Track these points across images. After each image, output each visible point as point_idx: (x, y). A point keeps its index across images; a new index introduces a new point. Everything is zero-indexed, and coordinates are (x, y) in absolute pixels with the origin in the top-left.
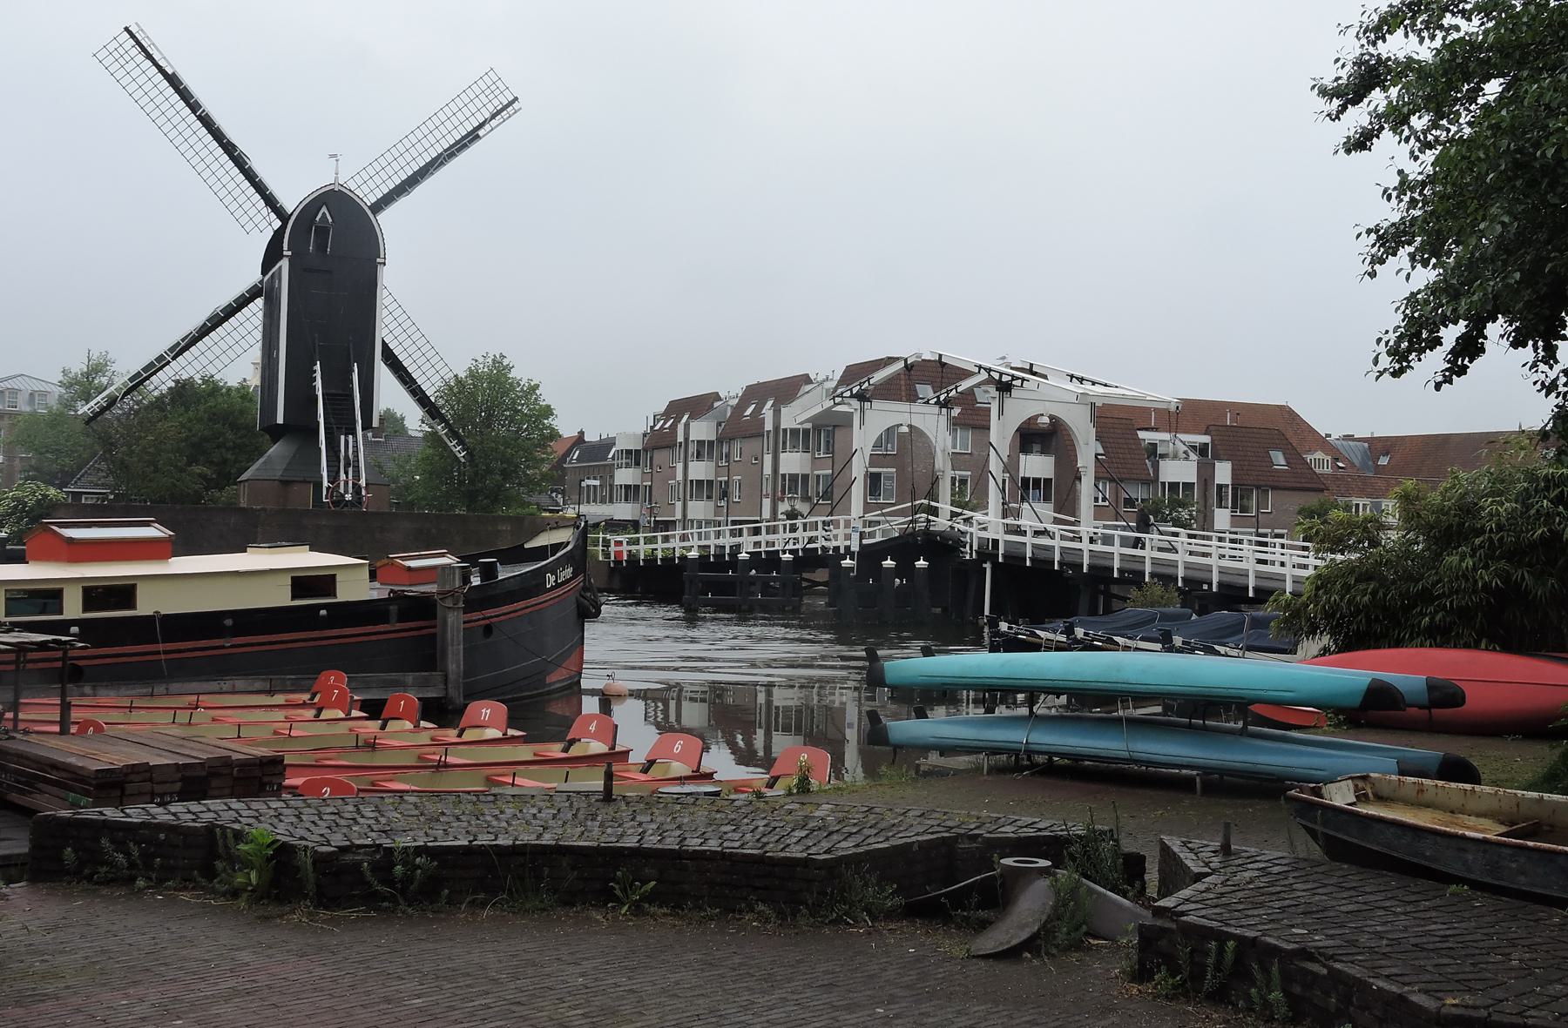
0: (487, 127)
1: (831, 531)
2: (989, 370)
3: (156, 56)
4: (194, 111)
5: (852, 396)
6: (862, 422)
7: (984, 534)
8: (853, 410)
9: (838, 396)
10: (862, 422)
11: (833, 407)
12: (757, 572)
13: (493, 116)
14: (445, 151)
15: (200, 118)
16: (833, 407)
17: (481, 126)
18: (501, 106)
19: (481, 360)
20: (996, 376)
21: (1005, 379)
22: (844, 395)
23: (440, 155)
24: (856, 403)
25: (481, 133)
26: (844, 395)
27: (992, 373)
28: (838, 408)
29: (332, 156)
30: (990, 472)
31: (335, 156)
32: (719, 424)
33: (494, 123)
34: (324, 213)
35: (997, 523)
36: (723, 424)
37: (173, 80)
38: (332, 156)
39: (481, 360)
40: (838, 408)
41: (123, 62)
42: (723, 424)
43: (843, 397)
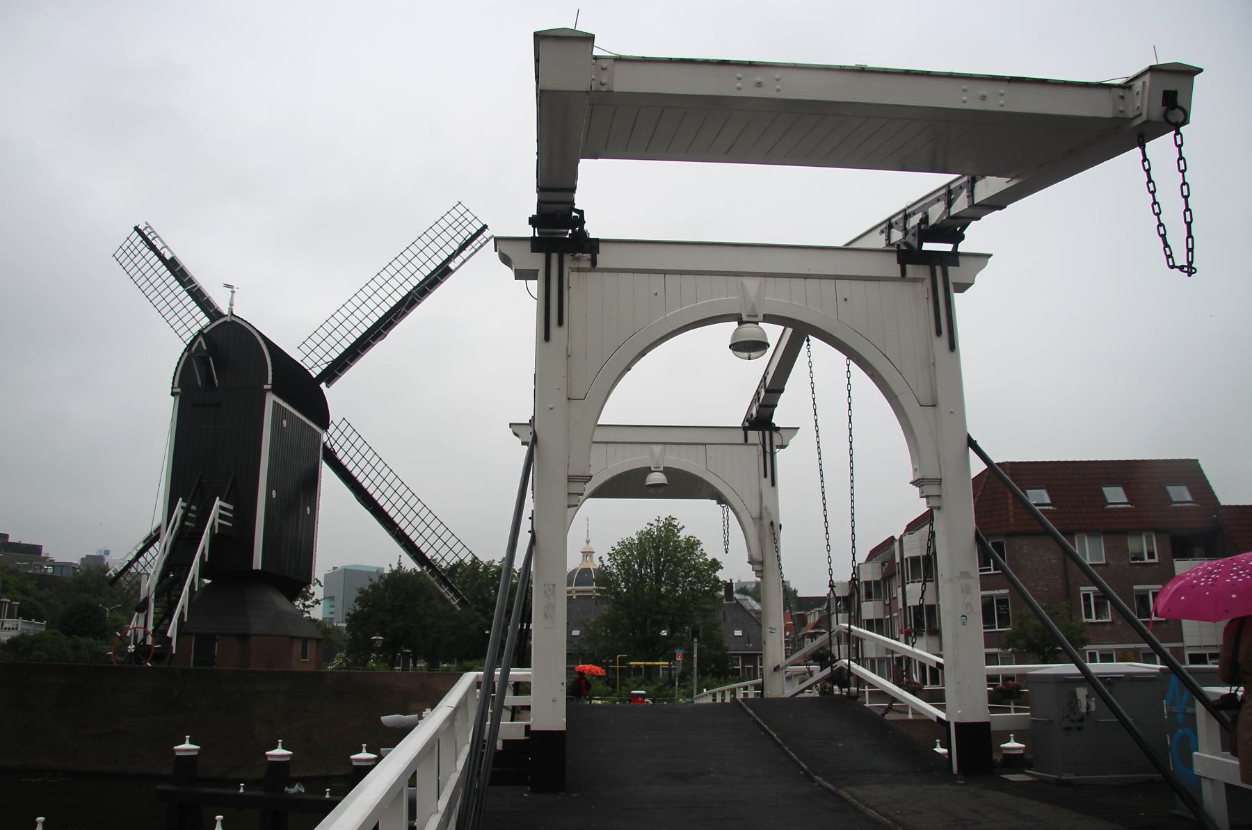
0: (458, 260)
3: (159, 246)
4: (183, 284)
13: (462, 248)
14: (415, 288)
15: (190, 293)
17: (451, 258)
18: (470, 236)
19: (655, 523)
23: (410, 293)
25: (452, 265)
29: (227, 286)
31: (231, 287)
32: (883, 564)
33: (465, 254)
34: (200, 342)
36: (887, 564)
37: (173, 265)
38: (227, 286)
39: (655, 523)
41: (132, 256)
42: (887, 564)
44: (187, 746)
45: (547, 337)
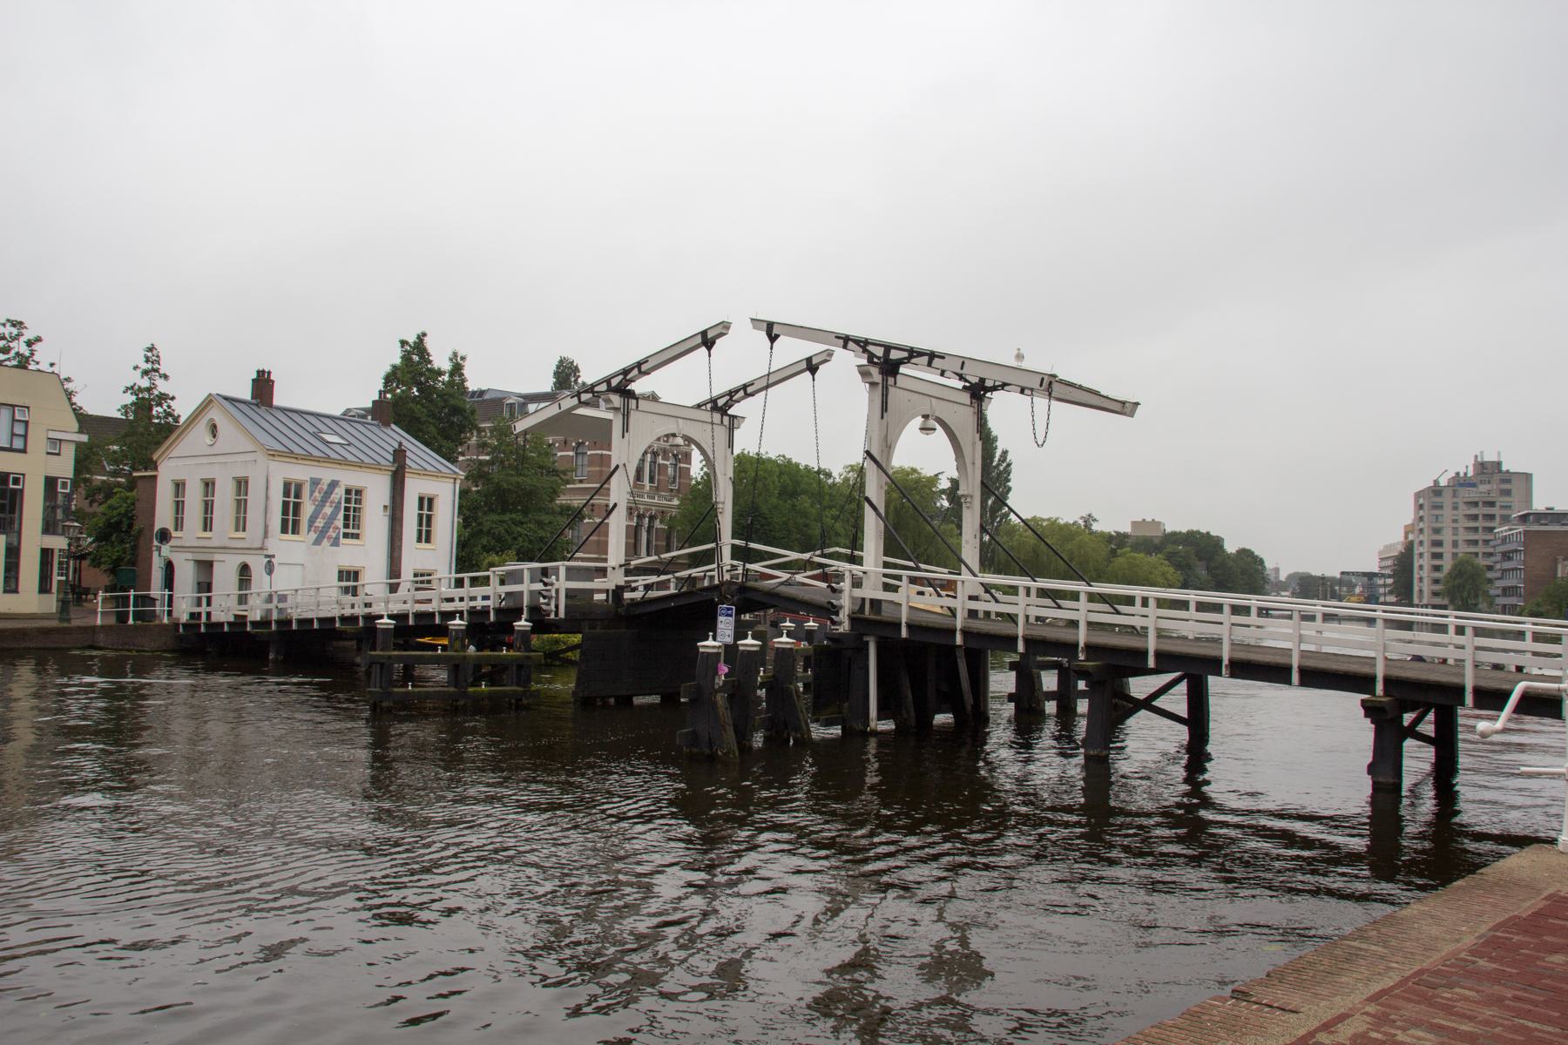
1: (552, 584)
2: (864, 344)
5: (611, 389)
6: (626, 428)
7: (858, 593)
8: (609, 415)
9: (586, 392)
10: (626, 428)
11: (575, 408)
12: (479, 649)
16: (575, 408)
20: (879, 352)
21: (895, 355)
22: (596, 389)
24: (616, 400)
26: (596, 389)
27: (870, 348)
28: (582, 411)
30: (868, 500)
35: (876, 573)
40: (582, 411)
43: (593, 392)
44: (811, 623)
45: (882, 417)
